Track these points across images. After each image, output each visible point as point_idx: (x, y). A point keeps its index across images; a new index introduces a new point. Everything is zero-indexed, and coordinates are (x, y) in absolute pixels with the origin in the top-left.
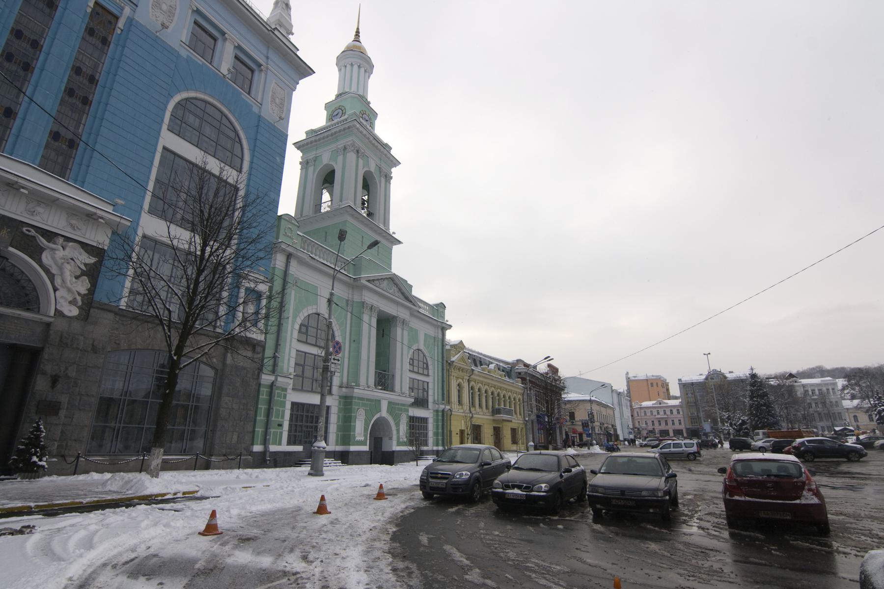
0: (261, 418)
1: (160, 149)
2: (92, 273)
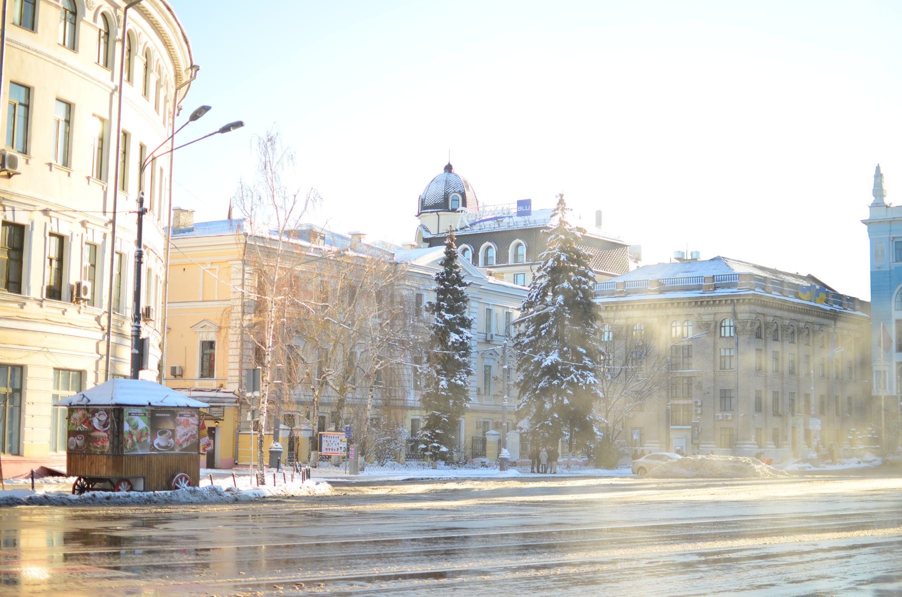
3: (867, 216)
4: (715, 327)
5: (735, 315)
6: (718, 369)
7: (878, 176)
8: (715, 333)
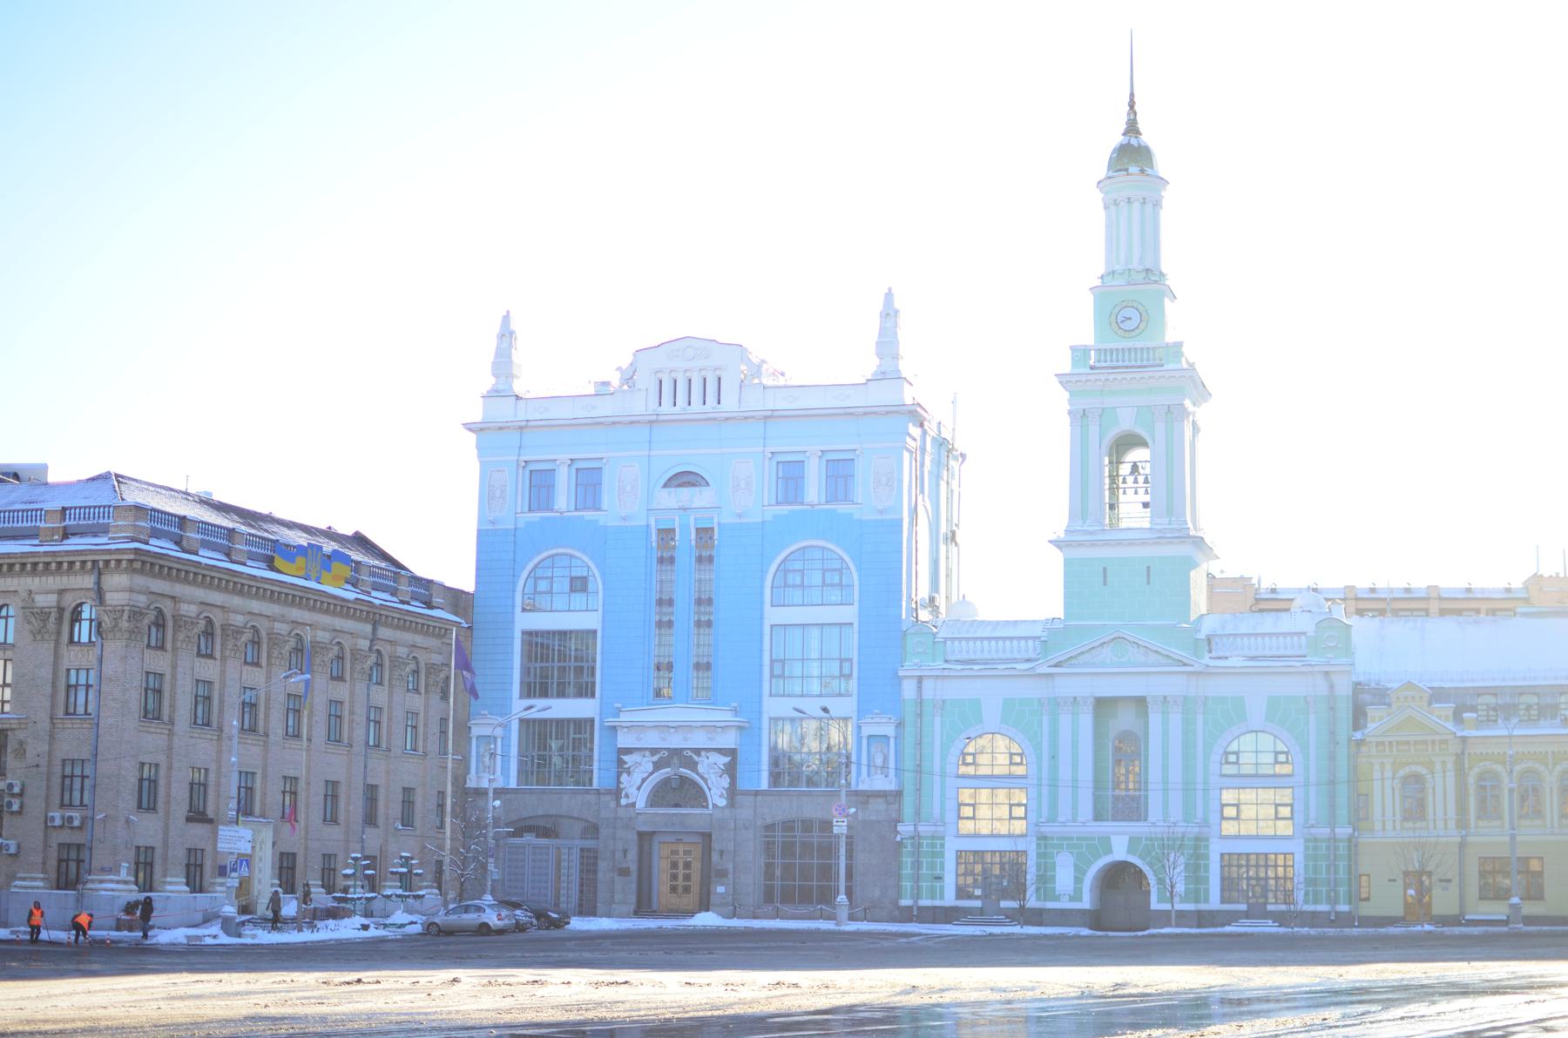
0: (907, 871)
1: (767, 630)
2: (731, 770)
3: (477, 416)
4: (60, 619)
5: (100, 593)
6: (60, 712)
7: (506, 335)
8: (59, 633)
